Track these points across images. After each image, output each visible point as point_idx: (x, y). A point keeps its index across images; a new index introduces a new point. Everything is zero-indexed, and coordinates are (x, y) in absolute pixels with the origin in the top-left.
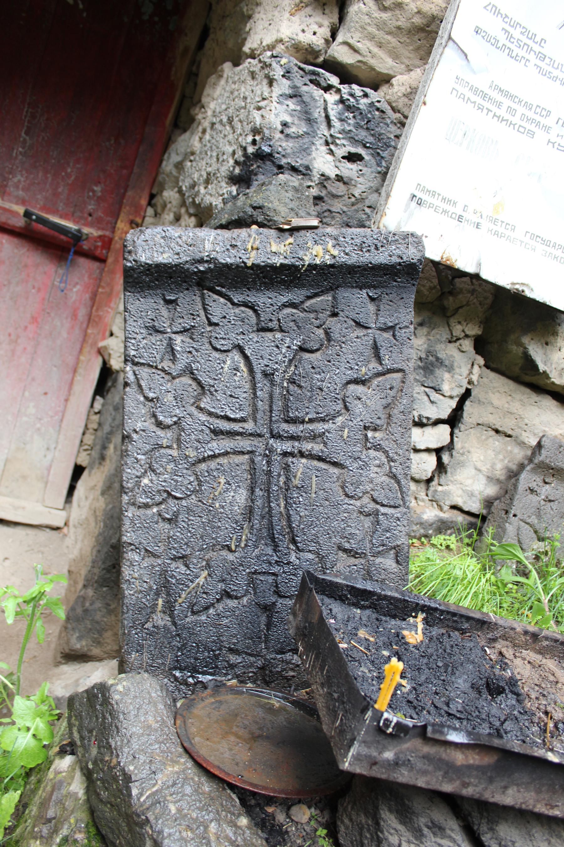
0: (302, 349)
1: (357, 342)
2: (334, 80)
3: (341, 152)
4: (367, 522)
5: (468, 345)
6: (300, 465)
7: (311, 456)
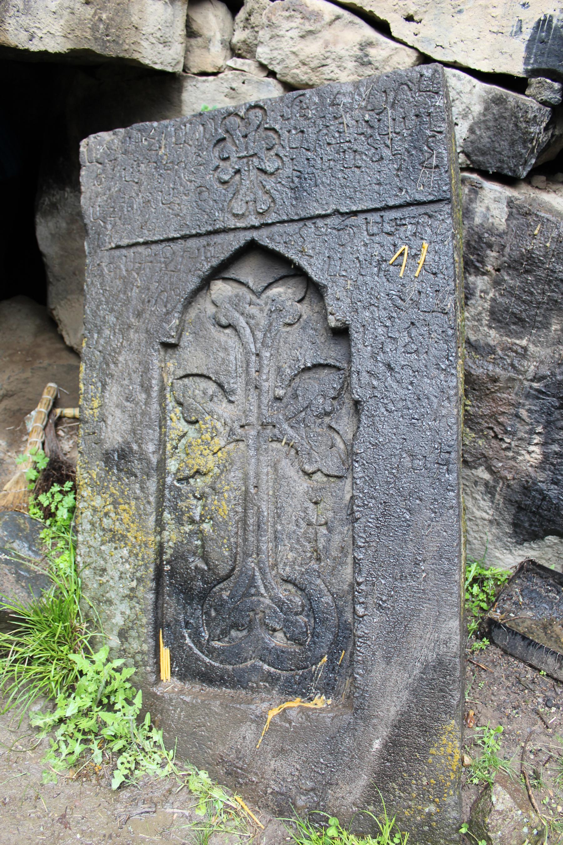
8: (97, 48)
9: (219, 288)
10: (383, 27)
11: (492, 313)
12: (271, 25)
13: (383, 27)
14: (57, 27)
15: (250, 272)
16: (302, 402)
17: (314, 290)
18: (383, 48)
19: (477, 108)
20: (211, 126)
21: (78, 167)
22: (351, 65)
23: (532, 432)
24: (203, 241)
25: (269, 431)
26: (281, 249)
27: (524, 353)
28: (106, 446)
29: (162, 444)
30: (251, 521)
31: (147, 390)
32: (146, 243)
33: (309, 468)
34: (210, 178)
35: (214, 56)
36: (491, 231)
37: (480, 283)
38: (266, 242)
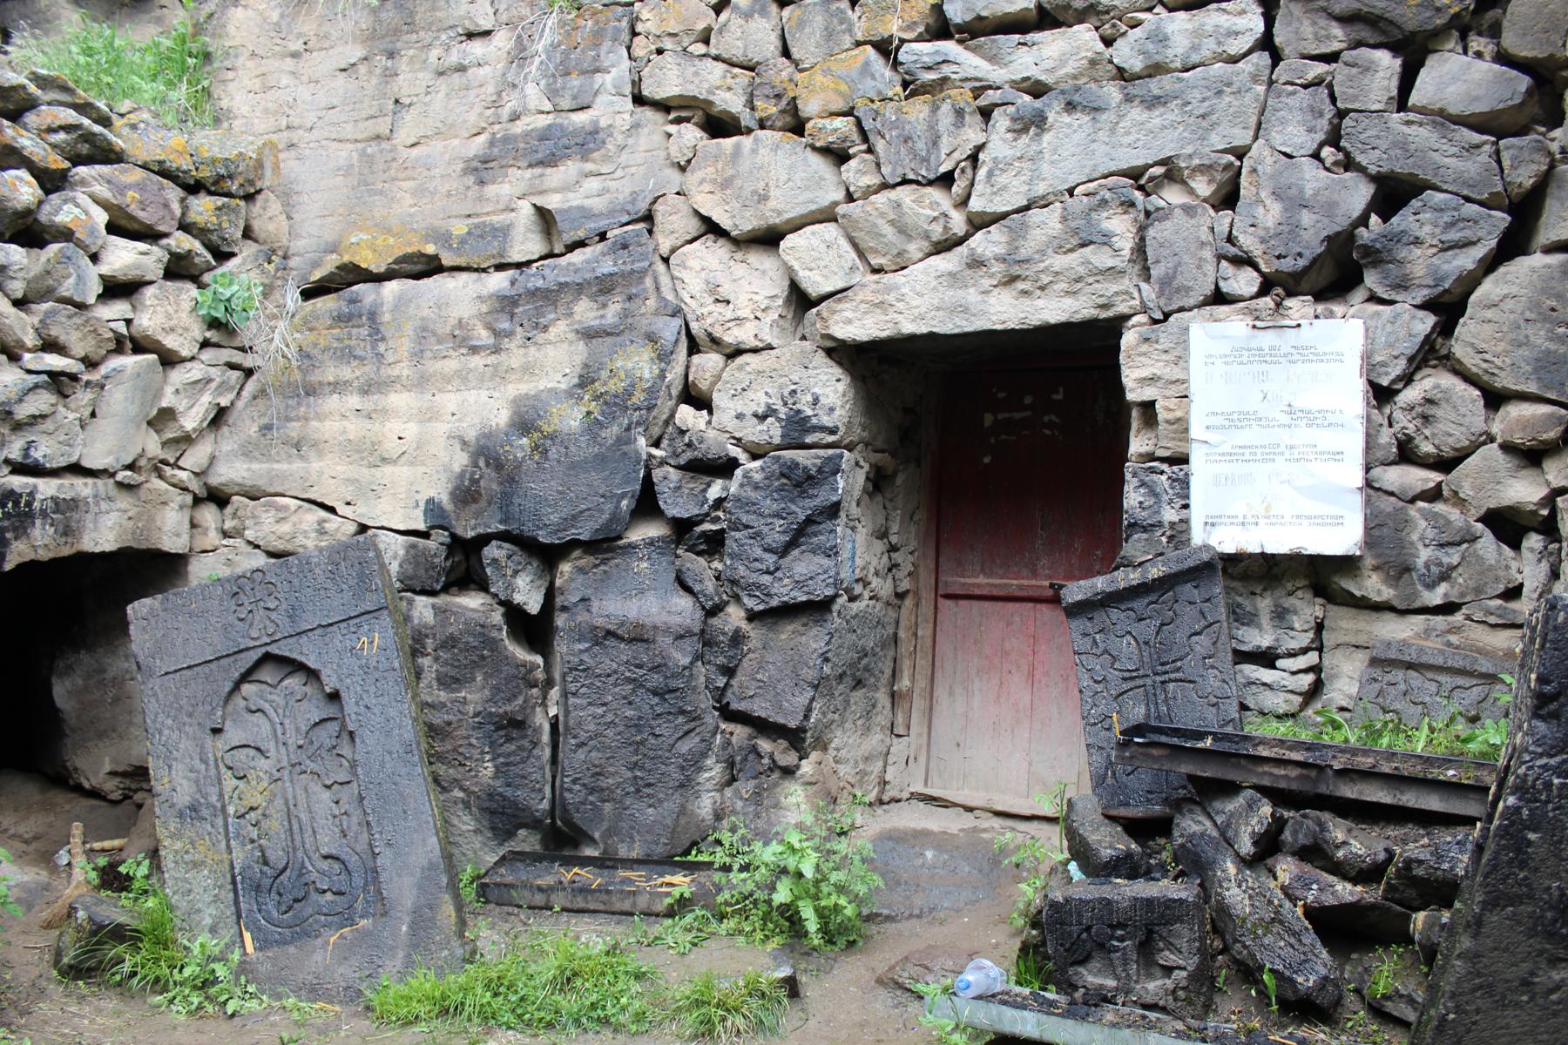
0: (1163, 625)
2: (1165, 467)
3: (1177, 506)
4: (1214, 710)
5: (1309, 595)
6: (1171, 686)
7: (1176, 680)
8: (135, 545)
9: (247, 688)
10: (332, 510)
11: (438, 679)
12: (254, 517)
13: (332, 510)
15: (268, 674)
17: (312, 675)
18: (333, 523)
19: (402, 552)
20: (227, 586)
22: (313, 535)
23: (483, 753)
24: (232, 659)
25: (298, 769)
26: (287, 654)
27: (465, 701)
28: (180, 806)
29: (221, 795)
30: (296, 827)
31: (207, 763)
32: (189, 667)
33: (328, 783)
35: (213, 538)
36: (425, 626)
37: (425, 662)
38: (277, 652)
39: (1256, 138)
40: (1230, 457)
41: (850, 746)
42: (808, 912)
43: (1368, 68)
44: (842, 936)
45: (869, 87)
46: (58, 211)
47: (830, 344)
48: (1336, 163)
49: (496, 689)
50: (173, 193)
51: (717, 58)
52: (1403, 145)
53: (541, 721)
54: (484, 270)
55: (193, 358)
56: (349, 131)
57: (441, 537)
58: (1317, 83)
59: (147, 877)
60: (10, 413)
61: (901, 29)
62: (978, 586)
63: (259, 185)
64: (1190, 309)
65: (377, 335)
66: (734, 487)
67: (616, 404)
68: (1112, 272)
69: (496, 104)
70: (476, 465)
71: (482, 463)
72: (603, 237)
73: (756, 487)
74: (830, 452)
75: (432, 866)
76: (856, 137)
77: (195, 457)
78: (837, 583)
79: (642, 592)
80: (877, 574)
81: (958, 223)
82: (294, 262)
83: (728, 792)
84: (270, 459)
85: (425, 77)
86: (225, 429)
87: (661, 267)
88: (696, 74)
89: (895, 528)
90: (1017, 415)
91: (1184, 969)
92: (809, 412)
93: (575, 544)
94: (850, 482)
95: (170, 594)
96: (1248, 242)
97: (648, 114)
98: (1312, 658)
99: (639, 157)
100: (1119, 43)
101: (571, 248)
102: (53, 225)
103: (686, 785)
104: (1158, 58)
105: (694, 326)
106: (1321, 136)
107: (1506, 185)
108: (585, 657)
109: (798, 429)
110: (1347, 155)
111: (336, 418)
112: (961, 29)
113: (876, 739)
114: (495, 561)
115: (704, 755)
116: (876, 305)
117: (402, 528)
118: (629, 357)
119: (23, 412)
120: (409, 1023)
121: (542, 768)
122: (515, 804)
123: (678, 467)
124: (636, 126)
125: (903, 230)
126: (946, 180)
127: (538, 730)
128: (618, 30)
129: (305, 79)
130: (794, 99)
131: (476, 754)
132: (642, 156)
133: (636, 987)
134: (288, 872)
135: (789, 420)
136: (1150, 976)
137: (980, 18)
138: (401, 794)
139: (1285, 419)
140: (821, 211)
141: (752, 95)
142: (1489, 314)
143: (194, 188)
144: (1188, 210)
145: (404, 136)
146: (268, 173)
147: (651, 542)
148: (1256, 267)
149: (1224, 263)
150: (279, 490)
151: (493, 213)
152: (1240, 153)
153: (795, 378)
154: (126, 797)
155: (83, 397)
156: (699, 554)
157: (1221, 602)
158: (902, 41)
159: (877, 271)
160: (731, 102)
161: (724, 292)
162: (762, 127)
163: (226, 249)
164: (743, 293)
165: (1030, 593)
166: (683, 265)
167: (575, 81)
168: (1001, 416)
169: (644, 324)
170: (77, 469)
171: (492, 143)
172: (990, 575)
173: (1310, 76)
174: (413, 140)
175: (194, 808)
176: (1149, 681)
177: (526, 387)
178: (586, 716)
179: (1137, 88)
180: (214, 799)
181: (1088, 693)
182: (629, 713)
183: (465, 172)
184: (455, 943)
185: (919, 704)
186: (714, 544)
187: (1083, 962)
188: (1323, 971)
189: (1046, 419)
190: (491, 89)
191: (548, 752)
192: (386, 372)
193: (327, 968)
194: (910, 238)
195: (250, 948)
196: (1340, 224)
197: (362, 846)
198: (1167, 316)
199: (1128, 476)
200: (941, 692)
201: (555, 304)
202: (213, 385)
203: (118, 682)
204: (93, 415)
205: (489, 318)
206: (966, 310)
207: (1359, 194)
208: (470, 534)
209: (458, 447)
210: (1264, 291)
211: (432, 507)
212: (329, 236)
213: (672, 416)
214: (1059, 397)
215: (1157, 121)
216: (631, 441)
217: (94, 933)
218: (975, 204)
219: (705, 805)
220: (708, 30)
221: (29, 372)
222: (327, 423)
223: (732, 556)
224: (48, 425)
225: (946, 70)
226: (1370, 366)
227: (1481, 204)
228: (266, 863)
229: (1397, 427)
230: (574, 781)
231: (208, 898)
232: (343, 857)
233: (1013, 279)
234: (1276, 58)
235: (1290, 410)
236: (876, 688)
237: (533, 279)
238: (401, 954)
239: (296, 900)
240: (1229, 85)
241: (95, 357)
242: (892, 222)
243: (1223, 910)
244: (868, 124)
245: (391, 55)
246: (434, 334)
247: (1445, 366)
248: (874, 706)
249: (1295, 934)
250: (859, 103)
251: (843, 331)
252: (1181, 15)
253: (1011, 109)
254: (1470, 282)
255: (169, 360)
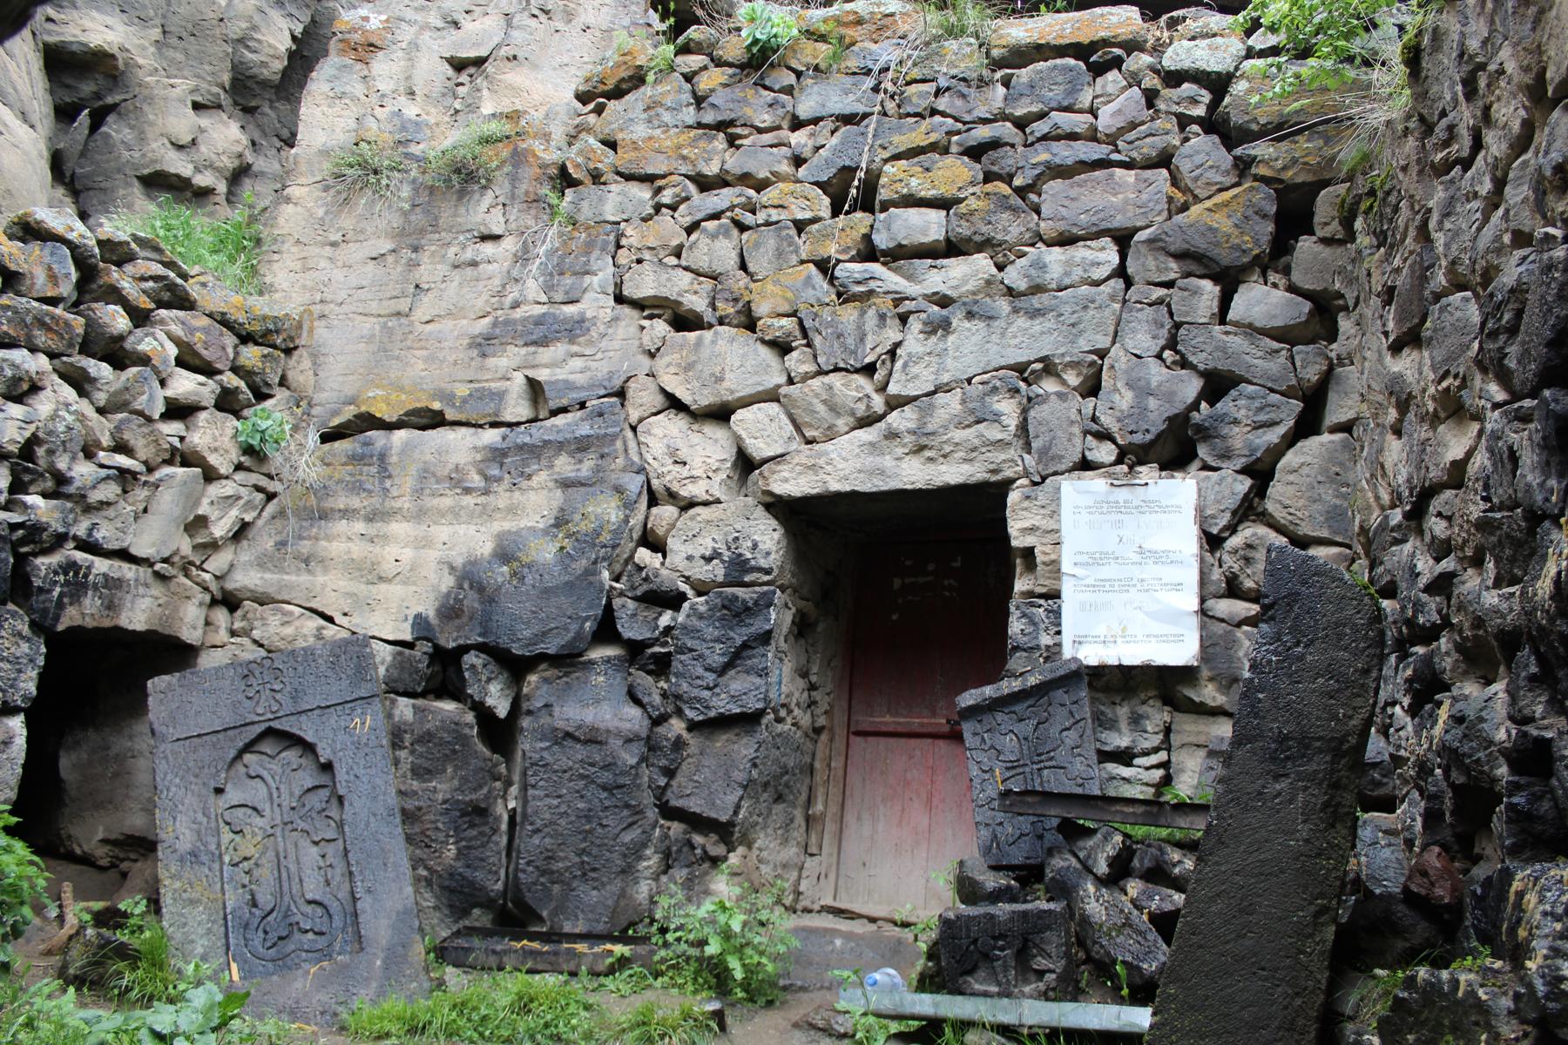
1: (1064, 712)
2: (1042, 602)
5: (1158, 704)
6: (1046, 772)
8: (160, 630)
9: (248, 757)
10: (330, 620)
11: (412, 770)
12: (262, 618)
13: (330, 620)
14: (143, 617)
15: (267, 747)
16: (308, 807)
17: (308, 748)
19: (389, 659)
21: (146, 695)
22: (312, 640)
23: (448, 836)
25: (290, 827)
27: (435, 790)
29: (219, 845)
30: (284, 875)
31: (209, 818)
32: (199, 736)
34: (241, 697)
35: (222, 636)
37: (403, 754)
39: (1114, 343)
40: (1094, 588)
41: (771, 848)
42: (734, 963)
43: (1196, 292)
44: (763, 993)
45: (809, 295)
46: (140, 341)
47: (769, 499)
48: (1174, 363)
49: (464, 780)
50: (230, 340)
51: (686, 269)
52: (1223, 349)
53: (501, 811)
54: (481, 426)
55: (227, 478)
56: (374, 307)
57: (427, 647)
58: (1159, 302)
59: (142, 915)
60: (84, 496)
61: (837, 252)
62: (885, 724)
63: (297, 342)
64: (1062, 473)
65: (384, 472)
66: (681, 618)
67: (588, 541)
68: (1001, 444)
69: (500, 294)
70: (461, 587)
71: (466, 586)
72: (582, 405)
73: (701, 617)
74: (765, 588)
75: (406, 912)
76: (797, 333)
77: (218, 562)
78: (766, 700)
79: (598, 702)
80: (798, 704)
81: (878, 403)
82: (316, 411)
83: (664, 879)
84: (282, 570)
85: (443, 269)
86: (245, 543)
87: (630, 434)
88: (669, 280)
89: (815, 669)
90: (922, 580)
91: (1053, 971)
92: (749, 556)
93: (543, 657)
94: (780, 617)
95: (187, 673)
96: (1108, 421)
97: (626, 310)
98: (1162, 756)
99: (616, 344)
100: (1009, 268)
101: (554, 413)
102: (135, 352)
103: (628, 871)
104: (1039, 281)
105: (655, 483)
106: (1162, 342)
107: (1299, 380)
108: (545, 754)
109: (739, 569)
110: (1183, 356)
111: (343, 540)
112: (885, 253)
113: (791, 852)
114: (473, 666)
115: (644, 845)
116: (808, 467)
117: (391, 638)
118: (599, 504)
119: (95, 497)
120: (379, 1038)
121: (499, 853)
122: (472, 884)
123: (635, 599)
124: (616, 319)
125: (833, 408)
126: (869, 370)
127: (498, 819)
128: (606, 243)
129: (340, 264)
130: (749, 302)
131: (441, 836)
132: (619, 344)
133: (583, 1014)
134: (274, 914)
135: (731, 562)
136: (1026, 982)
137: (900, 246)
138: (382, 850)
139: (1136, 558)
140: (766, 392)
141: (714, 298)
142: (1291, 478)
143: (246, 338)
144: (1060, 395)
145: (421, 314)
146: (305, 334)
147: (608, 660)
148: (1114, 441)
149: (1089, 437)
150: (286, 598)
151: (492, 380)
152: (1102, 354)
153: (738, 527)
154: (113, 866)
155: (141, 494)
156: (649, 673)
157: (1086, 701)
158: (839, 261)
159: (809, 442)
160: (697, 303)
161: (683, 454)
162: (721, 323)
163: (265, 390)
164: (702, 456)
165: (930, 730)
166: (648, 432)
167: (568, 280)
168: (908, 580)
169: (613, 478)
170: (124, 555)
171: (495, 324)
172: (897, 714)
173: (1154, 297)
174: (428, 318)
175: (194, 854)
176: (1027, 769)
177: (508, 525)
178: (542, 806)
179: (1022, 303)
180: (213, 847)
181: (976, 781)
182: (581, 805)
183: (470, 346)
184: (422, 976)
185: (830, 827)
186: (661, 666)
187: (970, 972)
188: (1163, 959)
189: (946, 582)
190: (497, 282)
191: (505, 840)
192: (390, 504)
193: (306, 994)
194: (838, 414)
195: (236, 977)
196: (1178, 408)
197: (343, 894)
198: (1044, 479)
199: (1012, 609)
200: (850, 818)
201: (539, 457)
202: (241, 502)
203: (120, 759)
204: (145, 511)
205: (482, 466)
206: (882, 473)
207: (1191, 387)
208: (452, 645)
209: (446, 571)
210: (1119, 461)
211: (420, 622)
212: (349, 391)
213: (632, 557)
214: (957, 564)
215: (1037, 328)
216: (596, 573)
217: (102, 947)
218: (893, 389)
219: (643, 890)
220: (680, 247)
221: (102, 466)
222: (335, 544)
223: (677, 675)
224: (111, 512)
225: (873, 284)
226: (1202, 519)
227: (1282, 394)
228: (255, 905)
229: (1225, 567)
230: (528, 863)
231: (200, 931)
232: (326, 902)
233: (922, 448)
234: (1129, 283)
235: (1141, 550)
236: (795, 807)
237: (522, 436)
238: (374, 984)
239: (281, 938)
240: (1093, 302)
241: (153, 464)
242: (824, 402)
243: (1085, 921)
244: (807, 324)
245: (416, 249)
246: (434, 475)
247: (1262, 522)
248: (792, 820)
249: (1140, 933)
250: (802, 307)
251: (779, 488)
252: (1057, 249)
253: (923, 316)
254: (1277, 452)
255: (210, 475)
